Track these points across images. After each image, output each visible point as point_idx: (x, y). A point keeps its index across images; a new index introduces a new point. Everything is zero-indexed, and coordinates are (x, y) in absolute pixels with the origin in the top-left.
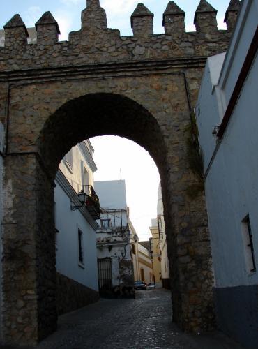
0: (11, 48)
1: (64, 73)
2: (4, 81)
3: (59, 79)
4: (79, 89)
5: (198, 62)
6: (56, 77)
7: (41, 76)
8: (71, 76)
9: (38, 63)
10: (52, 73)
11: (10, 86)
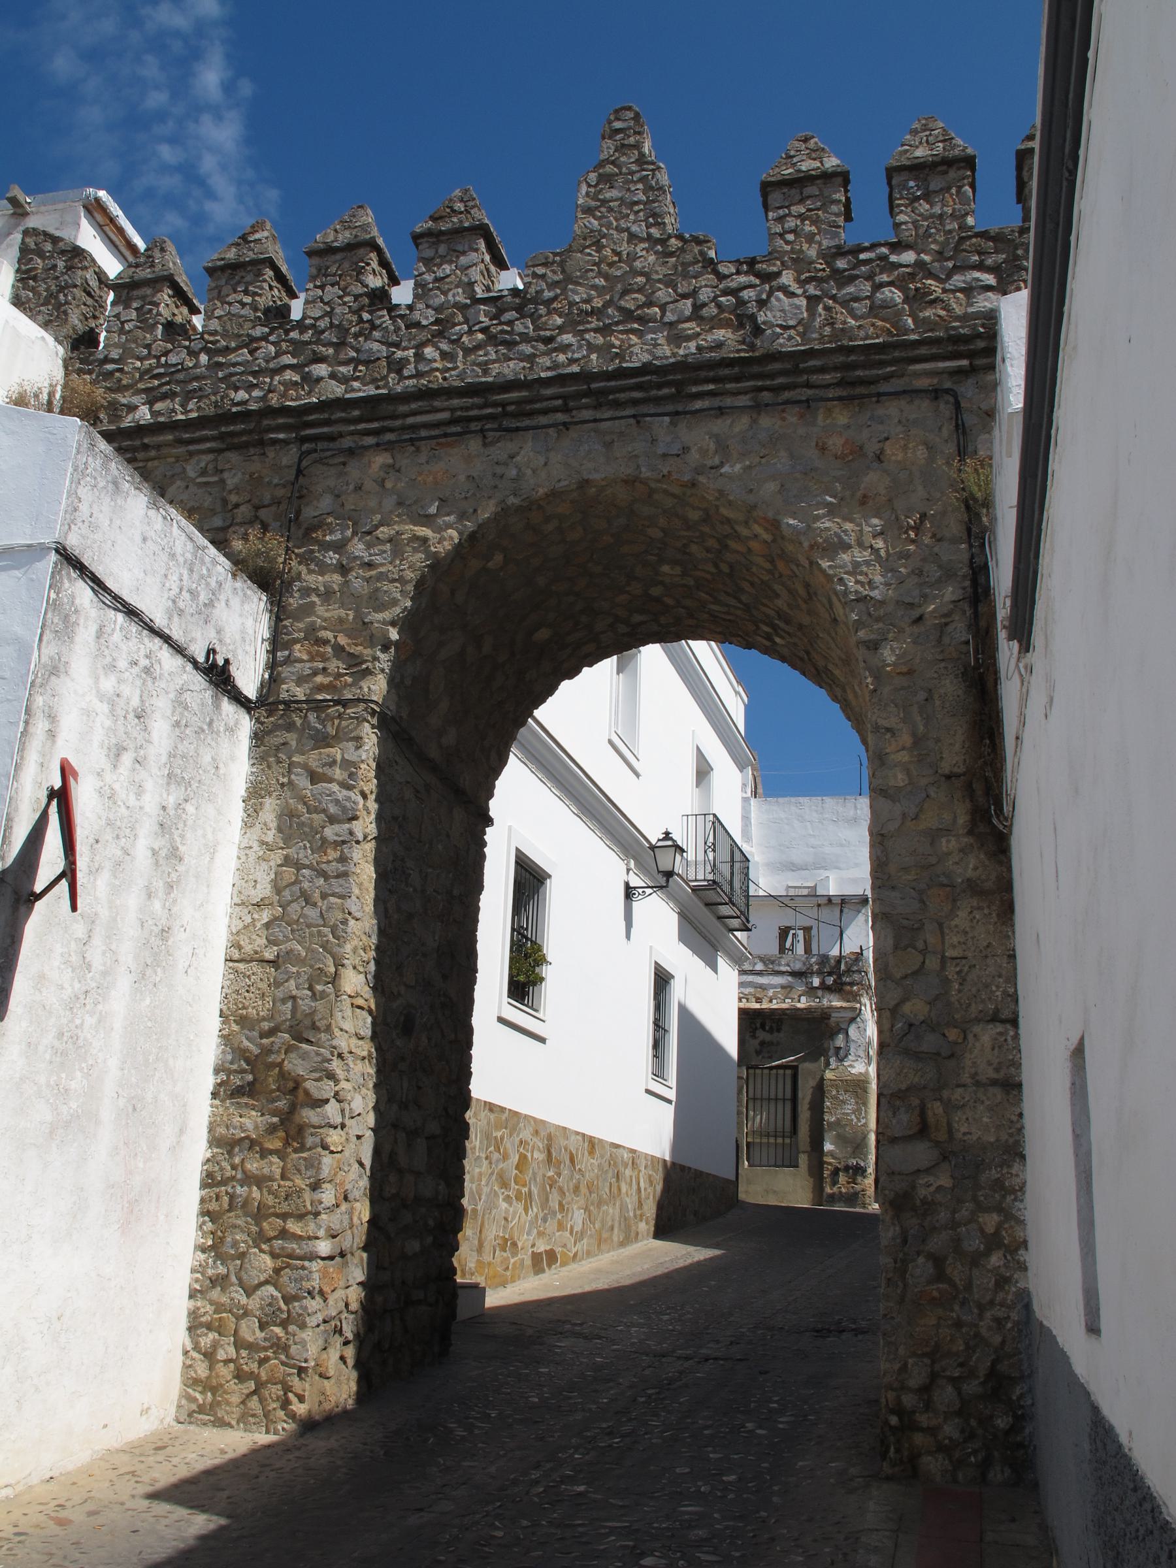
0: (322, 324)
1: (495, 404)
2: (285, 442)
3: (474, 426)
4: (543, 464)
5: (737, 379)
6: (470, 419)
7: (411, 420)
8: (514, 415)
9: (409, 370)
10: (453, 410)
11: (303, 455)
